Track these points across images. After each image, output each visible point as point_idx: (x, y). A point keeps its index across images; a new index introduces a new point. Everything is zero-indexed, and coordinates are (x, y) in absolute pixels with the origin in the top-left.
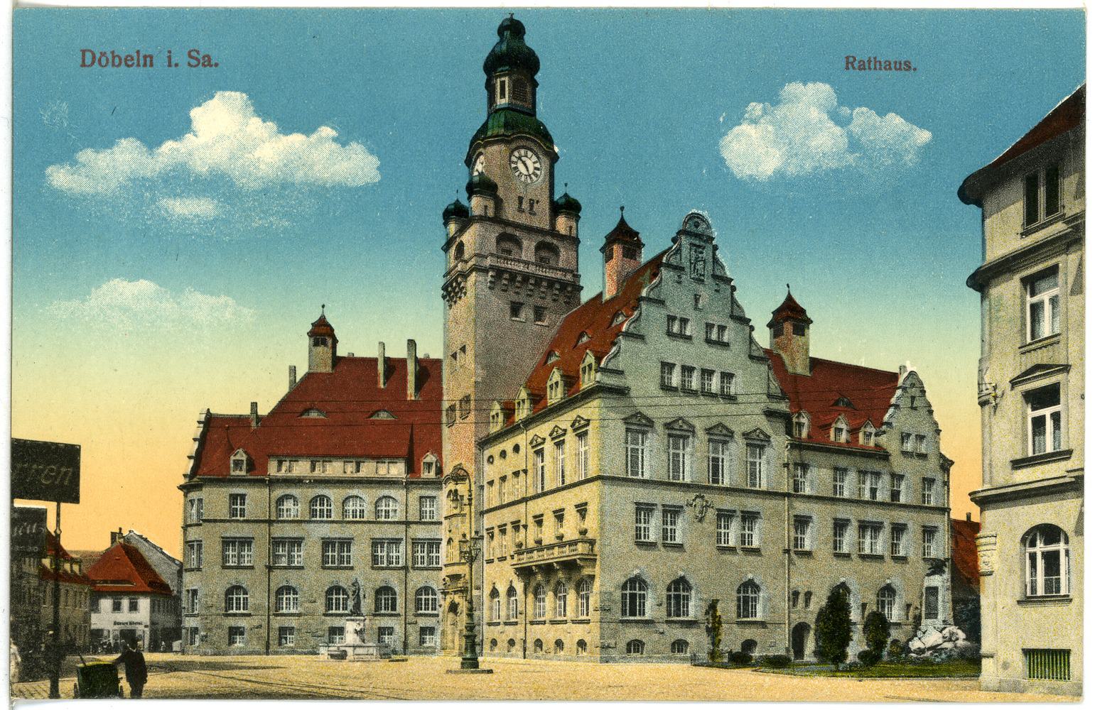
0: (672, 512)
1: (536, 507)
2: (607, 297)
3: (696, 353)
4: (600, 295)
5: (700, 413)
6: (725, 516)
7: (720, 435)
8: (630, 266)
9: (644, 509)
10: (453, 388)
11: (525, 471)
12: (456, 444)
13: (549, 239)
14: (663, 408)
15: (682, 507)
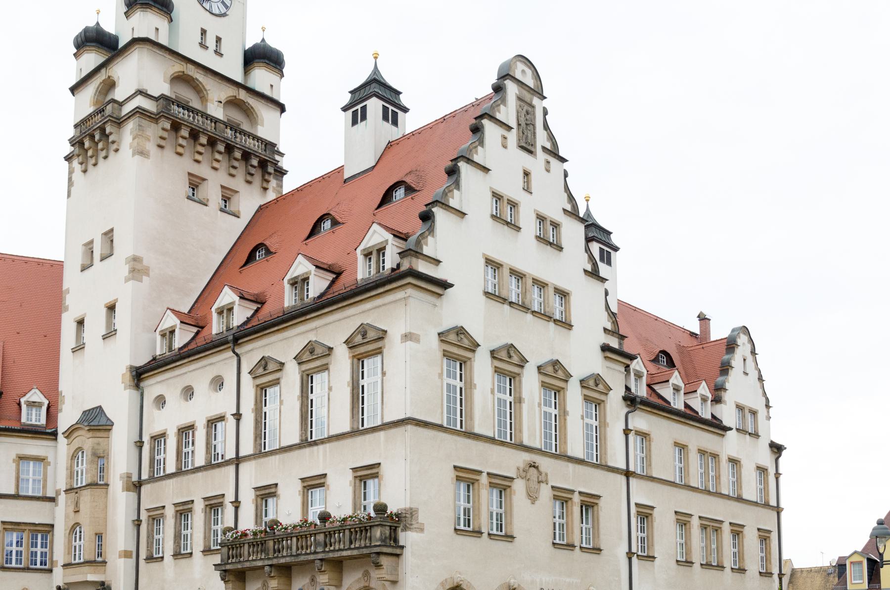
0: (501, 485)
1: (252, 476)
2: (347, 175)
3: (523, 252)
4: (340, 170)
5: (537, 343)
6: (562, 497)
7: (554, 375)
8: (391, 133)
9: (466, 477)
10: (83, 295)
11: (238, 416)
12: (93, 376)
13: (243, 95)
14: (490, 327)
15: (512, 479)
